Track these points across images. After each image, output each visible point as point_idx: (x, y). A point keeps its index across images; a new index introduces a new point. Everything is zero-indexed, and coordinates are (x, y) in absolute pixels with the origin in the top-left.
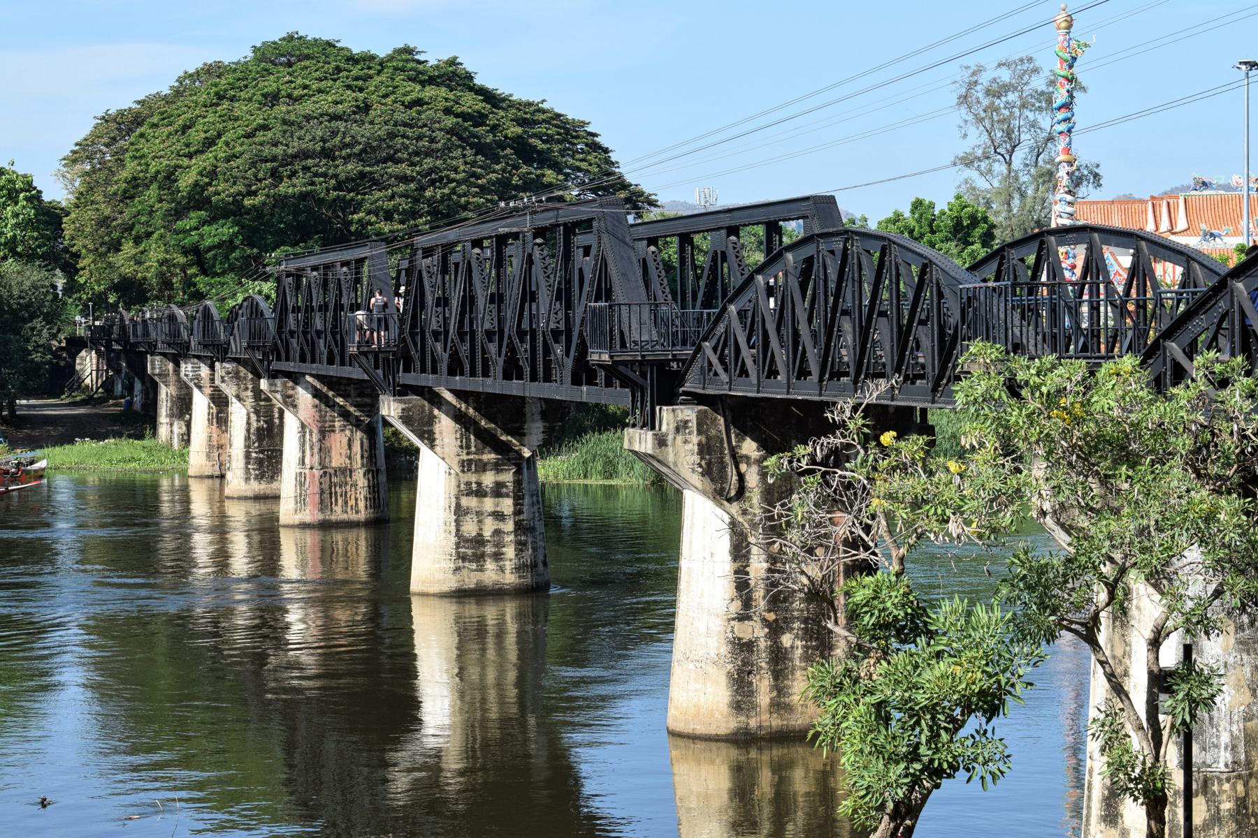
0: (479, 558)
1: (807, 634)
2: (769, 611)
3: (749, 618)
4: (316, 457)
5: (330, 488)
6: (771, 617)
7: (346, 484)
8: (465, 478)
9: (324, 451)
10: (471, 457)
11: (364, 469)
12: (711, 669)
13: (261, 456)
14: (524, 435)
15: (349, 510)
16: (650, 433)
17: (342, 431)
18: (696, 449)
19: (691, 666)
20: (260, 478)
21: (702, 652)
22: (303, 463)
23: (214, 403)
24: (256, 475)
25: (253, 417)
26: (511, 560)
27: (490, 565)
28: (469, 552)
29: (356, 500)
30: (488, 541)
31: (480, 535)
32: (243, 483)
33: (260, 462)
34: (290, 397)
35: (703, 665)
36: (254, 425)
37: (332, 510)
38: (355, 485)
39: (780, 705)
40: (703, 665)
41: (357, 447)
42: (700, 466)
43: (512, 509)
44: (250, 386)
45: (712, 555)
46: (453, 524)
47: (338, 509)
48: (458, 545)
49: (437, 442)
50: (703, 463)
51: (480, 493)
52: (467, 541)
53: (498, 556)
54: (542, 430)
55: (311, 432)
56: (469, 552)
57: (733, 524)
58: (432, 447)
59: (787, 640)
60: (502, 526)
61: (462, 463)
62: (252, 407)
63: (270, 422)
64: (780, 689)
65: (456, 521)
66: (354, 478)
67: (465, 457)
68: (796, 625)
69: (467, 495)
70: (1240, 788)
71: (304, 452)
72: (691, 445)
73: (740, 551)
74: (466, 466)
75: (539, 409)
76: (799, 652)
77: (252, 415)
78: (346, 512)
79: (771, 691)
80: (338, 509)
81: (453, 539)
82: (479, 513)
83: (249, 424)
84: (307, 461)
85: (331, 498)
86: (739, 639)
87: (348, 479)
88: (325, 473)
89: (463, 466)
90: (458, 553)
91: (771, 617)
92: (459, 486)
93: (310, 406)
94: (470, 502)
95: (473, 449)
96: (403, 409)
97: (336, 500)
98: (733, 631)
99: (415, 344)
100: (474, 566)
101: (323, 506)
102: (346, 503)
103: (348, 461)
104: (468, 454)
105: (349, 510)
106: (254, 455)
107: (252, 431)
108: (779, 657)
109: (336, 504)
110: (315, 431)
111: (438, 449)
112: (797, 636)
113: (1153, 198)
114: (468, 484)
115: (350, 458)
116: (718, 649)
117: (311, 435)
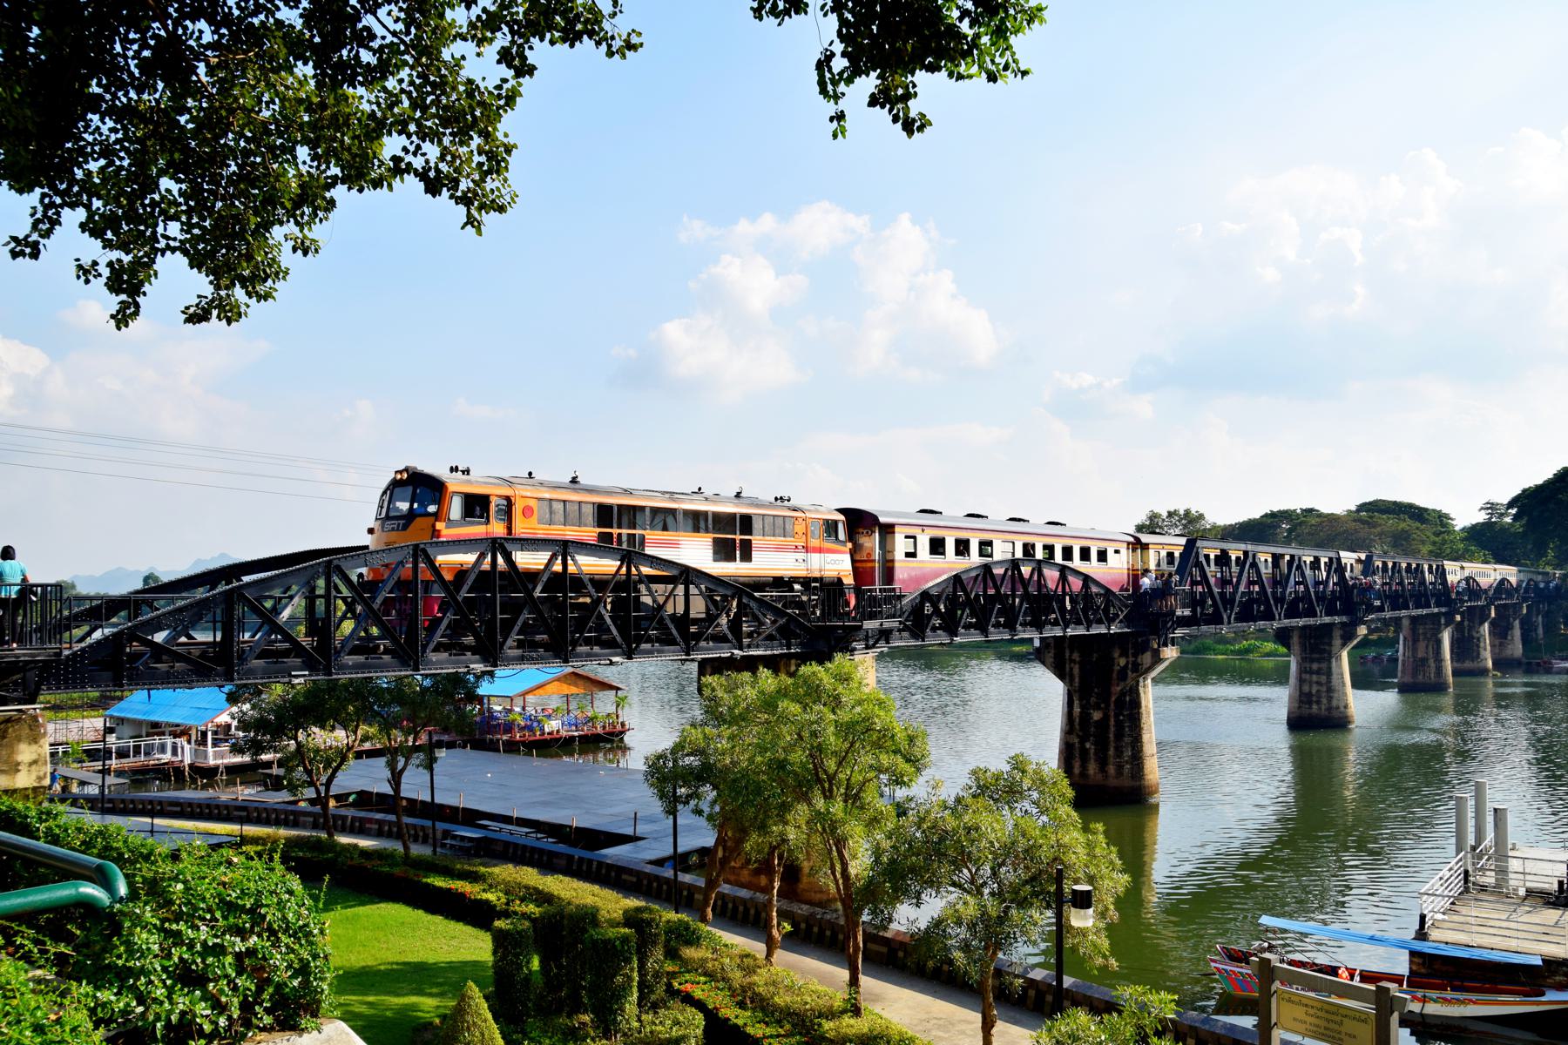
0: (1310, 703)
1: (1095, 744)
6: (1081, 734)
9: (1415, 650)
20: (1457, 661)
27: (1315, 707)
31: (1310, 692)
33: (1458, 654)
38: (1429, 667)
39: (1083, 774)
41: (1430, 648)
47: (1421, 677)
48: (1300, 696)
51: (1311, 672)
53: (1318, 702)
59: (1088, 745)
61: (1302, 658)
64: (1084, 767)
74: (1304, 659)
76: (1092, 751)
80: (1421, 677)
82: (1311, 683)
91: (1081, 734)
94: (1307, 676)
101: (1415, 674)
108: (1084, 754)
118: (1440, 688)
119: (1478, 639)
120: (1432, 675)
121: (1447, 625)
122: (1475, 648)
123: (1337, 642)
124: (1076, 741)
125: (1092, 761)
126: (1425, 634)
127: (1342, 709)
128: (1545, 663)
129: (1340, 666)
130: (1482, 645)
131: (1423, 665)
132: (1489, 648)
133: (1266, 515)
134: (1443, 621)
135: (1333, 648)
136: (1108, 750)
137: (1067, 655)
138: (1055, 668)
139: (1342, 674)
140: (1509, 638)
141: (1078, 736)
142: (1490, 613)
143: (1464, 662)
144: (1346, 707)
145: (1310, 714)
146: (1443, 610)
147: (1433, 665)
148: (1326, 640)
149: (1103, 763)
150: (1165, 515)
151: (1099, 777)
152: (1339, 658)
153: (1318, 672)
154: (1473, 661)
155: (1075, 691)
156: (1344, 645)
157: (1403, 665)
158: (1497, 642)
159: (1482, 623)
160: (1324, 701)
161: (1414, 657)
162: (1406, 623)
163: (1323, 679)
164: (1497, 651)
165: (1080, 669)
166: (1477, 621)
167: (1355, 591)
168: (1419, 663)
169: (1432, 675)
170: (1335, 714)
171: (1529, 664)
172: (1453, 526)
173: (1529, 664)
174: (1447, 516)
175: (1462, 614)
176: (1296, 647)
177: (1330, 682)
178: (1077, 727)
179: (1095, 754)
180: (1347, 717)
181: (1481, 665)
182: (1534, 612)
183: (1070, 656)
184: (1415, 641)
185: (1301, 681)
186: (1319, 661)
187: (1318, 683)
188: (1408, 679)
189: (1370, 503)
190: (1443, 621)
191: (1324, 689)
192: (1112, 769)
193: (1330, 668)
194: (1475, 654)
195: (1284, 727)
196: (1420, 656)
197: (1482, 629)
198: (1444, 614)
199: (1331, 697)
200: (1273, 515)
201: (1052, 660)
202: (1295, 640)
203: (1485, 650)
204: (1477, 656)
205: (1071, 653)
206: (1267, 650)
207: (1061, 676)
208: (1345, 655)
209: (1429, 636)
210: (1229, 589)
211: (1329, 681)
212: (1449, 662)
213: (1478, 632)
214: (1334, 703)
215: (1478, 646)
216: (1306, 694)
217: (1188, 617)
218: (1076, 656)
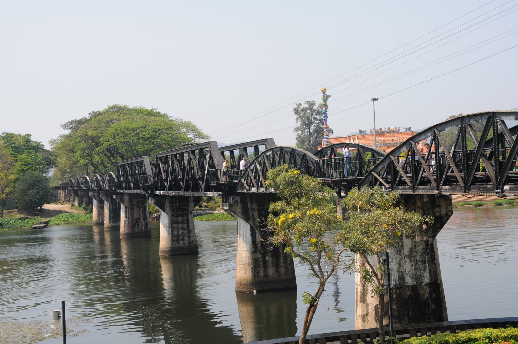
0: (178, 240)
1: (272, 256)
2: (262, 250)
3: (257, 253)
4: (130, 216)
5: (134, 223)
6: (263, 252)
7: (139, 222)
12: (247, 267)
16: (228, 204)
17: (137, 208)
18: (240, 207)
19: (242, 266)
20: (113, 222)
21: (244, 262)
22: (127, 218)
25: (111, 206)
27: (181, 242)
28: (175, 239)
29: (141, 226)
32: (109, 224)
35: (245, 266)
36: (111, 209)
39: (265, 276)
40: (245, 266)
42: (242, 212)
43: (186, 227)
44: (110, 197)
45: (246, 236)
48: (172, 237)
49: (166, 209)
50: (242, 211)
51: (178, 223)
52: (174, 236)
53: (183, 240)
54: (194, 205)
55: (128, 209)
57: (252, 228)
58: (164, 211)
59: (267, 258)
60: (184, 231)
63: (116, 207)
64: (265, 271)
65: (171, 231)
67: (173, 213)
68: (269, 254)
69: (174, 223)
70: (398, 291)
71: (126, 214)
72: (238, 207)
73: (253, 234)
74: (173, 216)
79: (263, 272)
80: (136, 230)
81: (171, 236)
82: (178, 229)
83: (110, 207)
84: (127, 217)
86: (254, 258)
88: (132, 220)
90: (172, 239)
91: (263, 252)
93: (128, 202)
94: (175, 225)
97: (136, 227)
98: (252, 256)
102: (139, 228)
104: (174, 212)
107: (111, 209)
108: (265, 262)
109: (136, 228)
110: (129, 208)
111: (166, 211)
112: (270, 257)
113: (348, 136)
115: (139, 215)
116: (249, 261)
120: (143, 228)
124: (260, 256)
125: (271, 267)
126: (137, 204)
127: (195, 242)
131: (137, 222)
135: (189, 207)
136: (279, 259)
137: (249, 205)
138: (242, 214)
141: (261, 253)
147: (143, 222)
149: (277, 266)
151: (276, 276)
153: (182, 222)
155: (257, 227)
160: (186, 238)
161: (132, 218)
165: (258, 213)
168: (135, 221)
176: (168, 209)
177: (189, 227)
178: (260, 248)
179: (272, 262)
183: (251, 206)
186: (182, 215)
187: (183, 229)
191: (186, 231)
192: (282, 270)
193: (188, 219)
196: (135, 217)
199: (190, 236)
201: (240, 210)
202: (167, 204)
205: (252, 204)
207: (247, 220)
209: (139, 205)
211: (188, 227)
214: (192, 239)
216: (176, 236)
217: (157, 190)
218: (255, 206)
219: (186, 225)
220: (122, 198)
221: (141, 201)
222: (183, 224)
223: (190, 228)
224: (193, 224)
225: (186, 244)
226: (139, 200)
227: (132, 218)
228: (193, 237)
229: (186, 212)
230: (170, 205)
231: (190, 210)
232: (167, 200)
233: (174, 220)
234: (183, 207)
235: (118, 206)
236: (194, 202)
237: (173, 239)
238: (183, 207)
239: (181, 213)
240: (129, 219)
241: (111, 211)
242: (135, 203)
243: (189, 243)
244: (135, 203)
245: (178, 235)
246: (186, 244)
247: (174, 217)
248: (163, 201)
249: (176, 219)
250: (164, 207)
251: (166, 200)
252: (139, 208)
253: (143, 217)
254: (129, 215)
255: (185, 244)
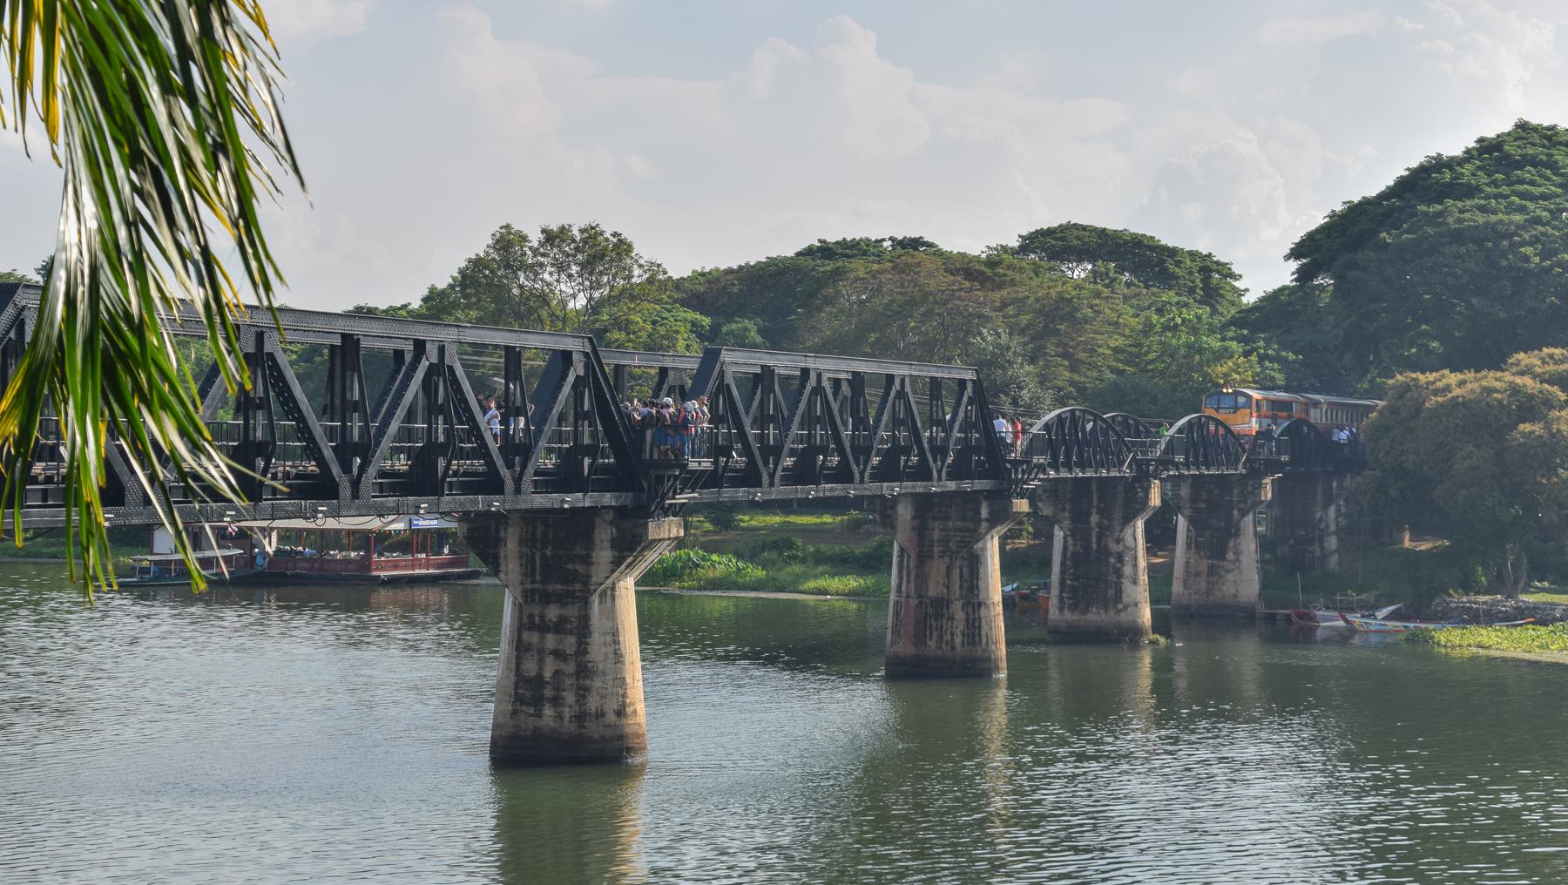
0: (537, 702)
4: (912, 585)
5: (926, 620)
7: (942, 616)
8: (527, 610)
9: (921, 579)
10: (536, 586)
11: (961, 602)
13: (1076, 583)
14: (592, 564)
15: (944, 645)
20: (1074, 607)
23: (1193, 526)
24: (1070, 605)
25: (1070, 541)
26: (570, 707)
27: (548, 711)
28: (528, 694)
29: (952, 634)
30: (548, 683)
31: (540, 676)
34: (889, 517)
37: (925, 644)
38: (951, 619)
43: (574, 648)
44: (1068, 507)
46: (514, 661)
48: (517, 685)
49: (502, 567)
51: (543, 628)
53: (556, 701)
54: (610, 559)
55: (909, 556)
56: (528, 694)
60: (563, 667)
61: (525, 593)
62: (1069, 530)
63: (1087, 547)
66: (951, 610)
67: (529, 586)
74: (528, 596)
75: (610, 537)
77: (1069, 538)
78: (941, 648)
80: (932, 644)
81: (513, 678)
83: (1065, 547)
84: (903, 588)
85: (925, 630)
87: (945, 611)
88: (920, 602)
89: (526, 596)
92: (521, 618)
93: (908, 528)
94: (532, 637)
95: (538, 578)
96: (469, 529)
97: (931, 634)
99: (766, 464)
100: (532, 711)
101: (920, 638)
102: (941, 637)
103: (945, 591)
104: (532, 583)
105: (944, 645)
106: (1069, 582)
107: (1068, 554)
109: (931, 638)
110: (913, 556)
114: (531, 616)
115: (948, 588)
117: (908, 561)
118: (974, 670)
119: (1120, 557)
120: (958, 640)
121: (994, 522)
122: (1113, 578)
123: (604, 555)
126: (945, 541)
127: (611, 718)
128: (1301, 616)
129: (612, 615)
130: (1127, 570)
131: (938, 616)
132: (1144, 578)
133: (809, 252)
134: (984, 512)
135: (593, 569)
139: (615, 634)
140: (1230, 556)
142: (1147, 498)
143: (1086, 610)
144: (621, 713)
145: (536, 729)
146: (980, 484)
147: (960, 615)
148: (579, 551)
150: (535, 238)
152: (610, 594)
153: (559, 627)
154: (1106, 609)
156: (617, 563)
157: (897, 613)
158: (1203, 566)
159: (1128, 519)
160: (570, 697)
162: (904, 512)
163: (570, 643)
164: (1203, 586)
166: (1118, 514)
167: (649, 433)
168: (930, 611)
169: (958, 640)
170: (593, 729)
171: (1271, 618)
172: (1240, 293)
173: (1271, 618)
174: (1227, 273)
175: (1032, 497)
176: (512, 565)
177: (586, 652)
180: (621, 737)
181: (1124, 617)
182: (1319, 499)
184: (924, 557)
185: (520, 648)
186: (562, 599)
187: (558, 654)
188: (905, 648)
189: (1049, 232)
190: (984, 512)
191: (570, 668)
193: (585, 619)
194: (1111, 592)
195: (484, 760)
196: (932, 593)
197: (1128, 531)
198: (989, 495)
199: (587, 689)
200: (825, 251)
202: (511, 548)
203: (1135, 582)
204: (1115, 598)
206: (720, 571)
208: (627, 588)
209: (952, 545)
210: (771, 431)
211: (582, 649)
212: (1000, 609)
213: (1118, 541)
214: (593, 703)
215: (1119, 574)
216: (528, 681)
219: (572, 640)
220: (889, 512)
221: (960, 530)
222: (559, 636)
223: (589, 657)
224: (609, 639)
225: (567, 719)
226: (950, 524)
227: (920, 596)
228: (603, 697)
229: (578, 586)
230: (520, 552)
231: (594, 579)
232: (510, 529)
233: (531, 616)
234: (570, 567)
235: (1094, 546)
236: (613, 547)
237: (521, 691)
238: (570, 567)
239: (558, 586)
240: (908, 597)
241: (1069, 563)
242: (936, 537)
243: (581, 717)
244: (936, 537)
245: (538, 681)
246: (567, 719)
247: (532, 601)
248: (497, 531)
249: (537, 612)
250: (496, 557)
251: (506, 530)
252: (951, 558)
253: (962, 597)
254: (908, 582)
255: (562, 718)
